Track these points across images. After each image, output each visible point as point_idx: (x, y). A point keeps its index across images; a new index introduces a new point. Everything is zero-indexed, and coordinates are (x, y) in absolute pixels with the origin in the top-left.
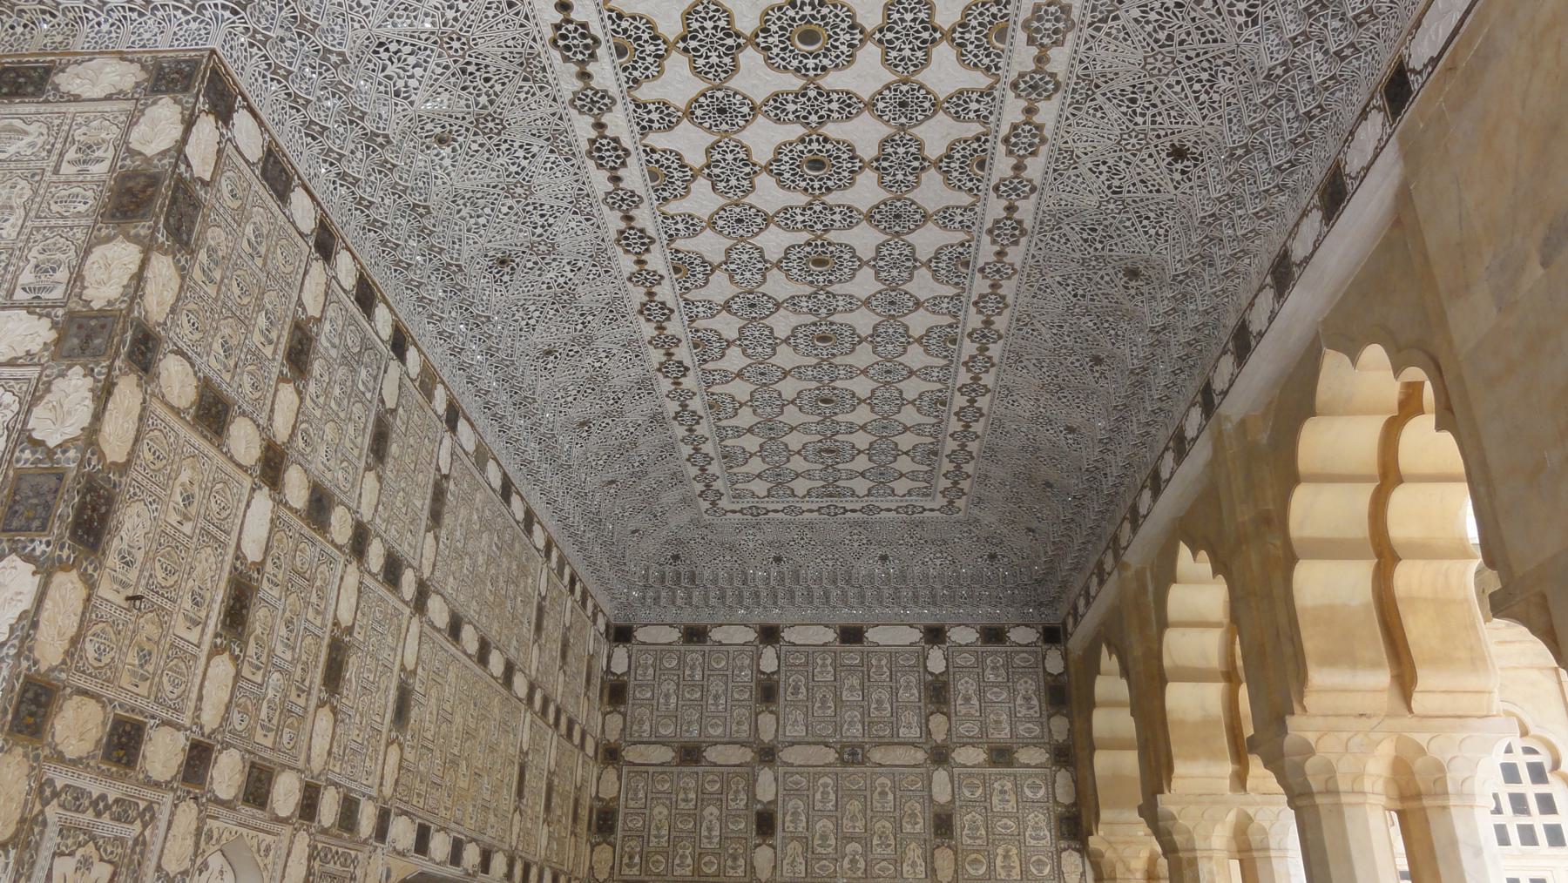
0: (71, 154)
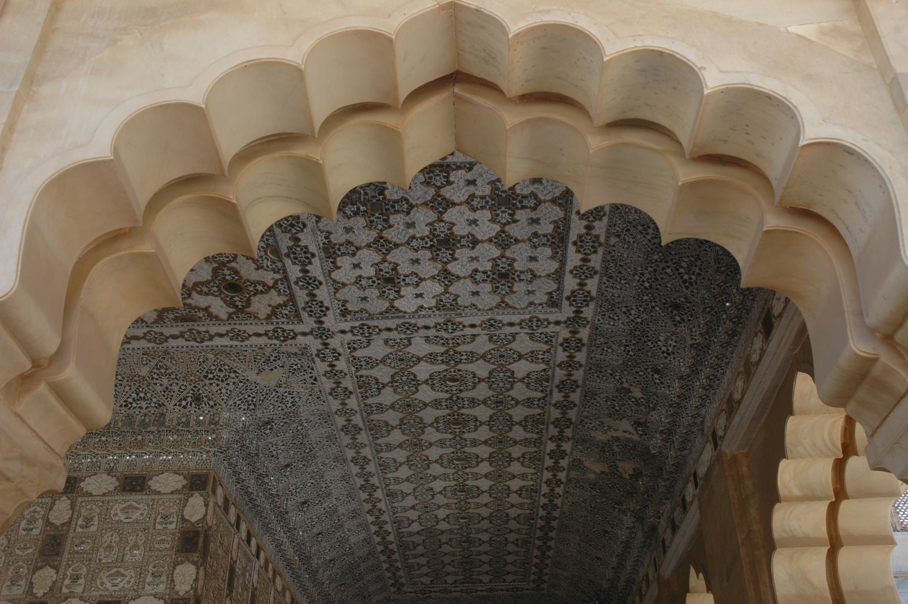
0: (159, 519)
